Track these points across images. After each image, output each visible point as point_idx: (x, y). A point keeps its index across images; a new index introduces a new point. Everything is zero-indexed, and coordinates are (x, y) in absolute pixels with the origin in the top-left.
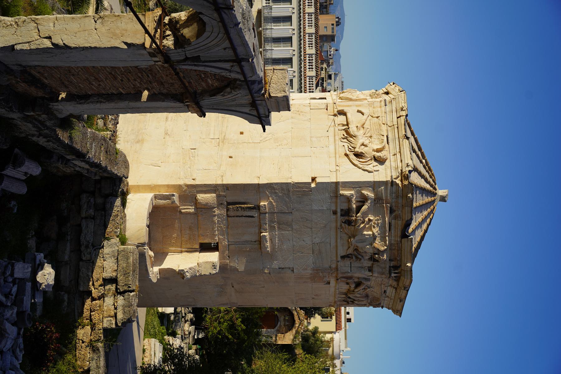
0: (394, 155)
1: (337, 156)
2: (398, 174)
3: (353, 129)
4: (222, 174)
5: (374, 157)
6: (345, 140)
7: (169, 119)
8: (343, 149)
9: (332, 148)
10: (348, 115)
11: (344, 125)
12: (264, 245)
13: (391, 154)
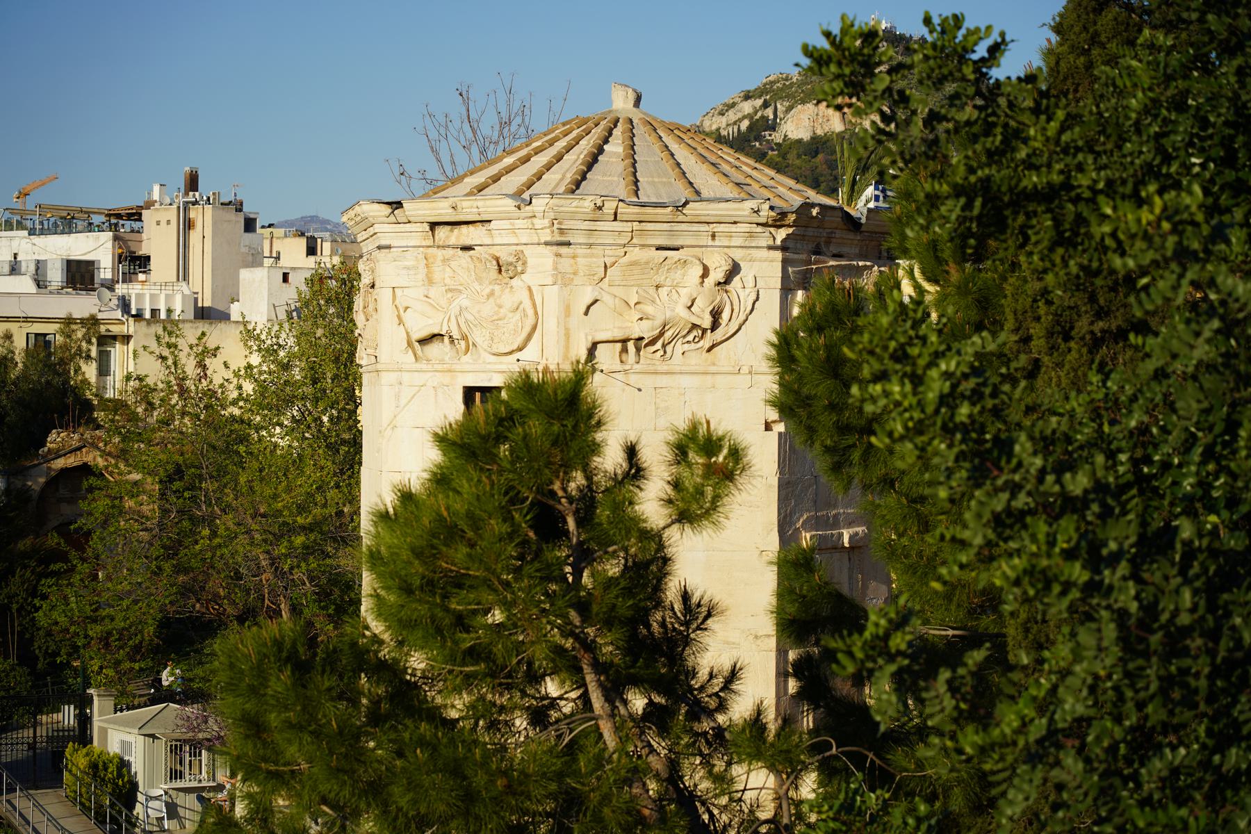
0: (713, 236)
1: (713, 369)
2: (767, 234)
3: (646, 330)
4: (751, 638)
5: (719, 283)
6: (669, 349)
8: (693, 354)
9: (686, 381)
10: (599, 338)
12: (861, 539)
13: (710, 243)
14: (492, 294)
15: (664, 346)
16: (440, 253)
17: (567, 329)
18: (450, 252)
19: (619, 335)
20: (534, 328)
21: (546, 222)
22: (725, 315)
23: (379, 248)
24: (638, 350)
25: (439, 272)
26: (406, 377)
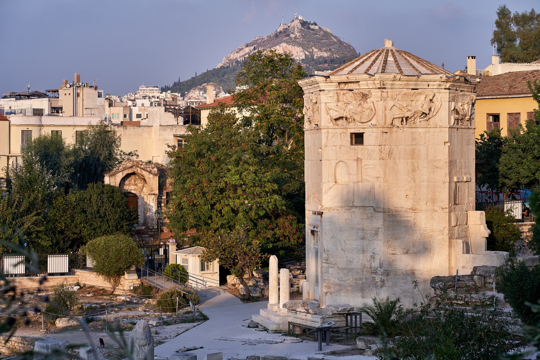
0: (428, 86)
1: (429, 126)
6: (416, 120)
7: (394, 252)
9: (421, 130)
11: (402, 121)
14: (360, 104)
15: (414, 119)
16: (342, 92)
17: (385, 115)
18: (345, 92)
19: (401, 116)
20: (375, 114)
21: (379, 82)
22: (432, 110)
23: (320, 91)
24: (407, 121)
25: (341, 98)
26: (330, 131)
